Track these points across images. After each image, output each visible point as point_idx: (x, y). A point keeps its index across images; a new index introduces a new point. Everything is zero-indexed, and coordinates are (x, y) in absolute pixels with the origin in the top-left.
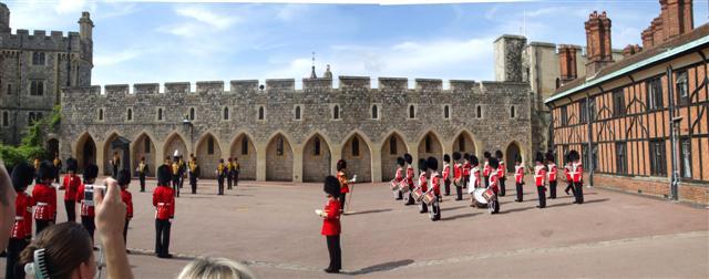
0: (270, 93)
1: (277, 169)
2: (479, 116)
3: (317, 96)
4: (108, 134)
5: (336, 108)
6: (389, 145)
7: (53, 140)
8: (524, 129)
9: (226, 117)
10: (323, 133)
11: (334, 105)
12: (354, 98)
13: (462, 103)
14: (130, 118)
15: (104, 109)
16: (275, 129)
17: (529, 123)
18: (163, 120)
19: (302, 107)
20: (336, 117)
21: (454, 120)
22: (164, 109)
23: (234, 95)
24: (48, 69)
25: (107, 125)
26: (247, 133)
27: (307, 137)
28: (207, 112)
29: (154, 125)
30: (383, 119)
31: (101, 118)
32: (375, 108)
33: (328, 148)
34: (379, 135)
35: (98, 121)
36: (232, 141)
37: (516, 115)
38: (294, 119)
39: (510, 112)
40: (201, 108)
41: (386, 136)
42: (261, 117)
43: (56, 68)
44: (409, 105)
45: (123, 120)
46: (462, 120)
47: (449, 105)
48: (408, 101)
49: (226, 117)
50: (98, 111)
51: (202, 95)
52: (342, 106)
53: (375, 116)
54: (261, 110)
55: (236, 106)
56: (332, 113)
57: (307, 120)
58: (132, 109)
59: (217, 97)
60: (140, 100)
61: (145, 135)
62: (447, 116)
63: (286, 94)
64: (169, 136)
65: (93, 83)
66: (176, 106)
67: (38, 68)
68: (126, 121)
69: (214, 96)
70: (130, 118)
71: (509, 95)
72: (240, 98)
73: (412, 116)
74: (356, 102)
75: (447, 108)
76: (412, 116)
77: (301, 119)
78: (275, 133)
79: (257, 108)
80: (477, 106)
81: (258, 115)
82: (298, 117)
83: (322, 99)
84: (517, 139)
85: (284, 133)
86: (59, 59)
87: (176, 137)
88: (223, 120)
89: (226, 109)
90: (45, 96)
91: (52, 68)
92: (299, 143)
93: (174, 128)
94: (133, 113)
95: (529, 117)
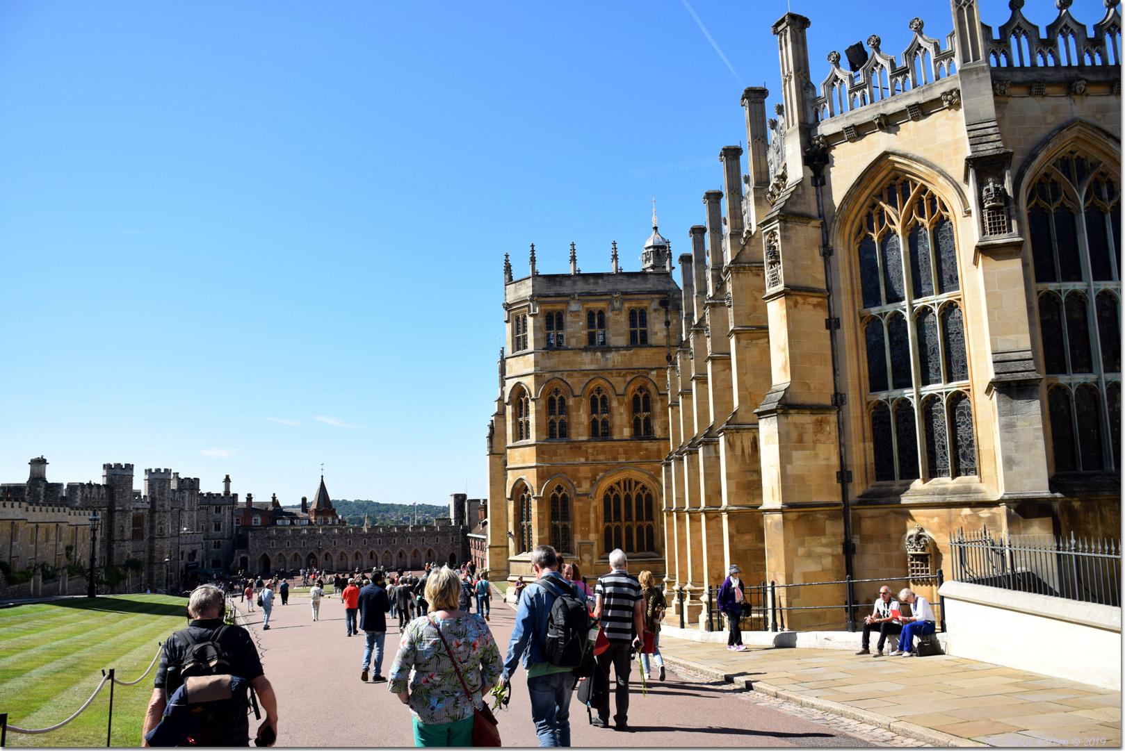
0: (353, 534)
4: (277, 554)
7: (244, 557)
8: (457, 547)
9: (335, 544)
10: (375, 550)
14: (288, 545)
15: (274, 542)
18: (306, 546)
19: (367, 540)
21: (426, 544)
24: (224, 515)
25: (276, 549)
27: (369, 552)
31: (273, 545)
40: (323, 541)
41: (398, 551)
48: (407, 536)
49: (335, 544)
62: (423, 542)
63: (360, 535)
65: (99, 478)
70: (288, 545)
73: (409, 542)
76: (409, 542)
79: (348, 540)
84: (454, 552)
85: (359, 551)
89: (335, 542)
90: (222, 531)
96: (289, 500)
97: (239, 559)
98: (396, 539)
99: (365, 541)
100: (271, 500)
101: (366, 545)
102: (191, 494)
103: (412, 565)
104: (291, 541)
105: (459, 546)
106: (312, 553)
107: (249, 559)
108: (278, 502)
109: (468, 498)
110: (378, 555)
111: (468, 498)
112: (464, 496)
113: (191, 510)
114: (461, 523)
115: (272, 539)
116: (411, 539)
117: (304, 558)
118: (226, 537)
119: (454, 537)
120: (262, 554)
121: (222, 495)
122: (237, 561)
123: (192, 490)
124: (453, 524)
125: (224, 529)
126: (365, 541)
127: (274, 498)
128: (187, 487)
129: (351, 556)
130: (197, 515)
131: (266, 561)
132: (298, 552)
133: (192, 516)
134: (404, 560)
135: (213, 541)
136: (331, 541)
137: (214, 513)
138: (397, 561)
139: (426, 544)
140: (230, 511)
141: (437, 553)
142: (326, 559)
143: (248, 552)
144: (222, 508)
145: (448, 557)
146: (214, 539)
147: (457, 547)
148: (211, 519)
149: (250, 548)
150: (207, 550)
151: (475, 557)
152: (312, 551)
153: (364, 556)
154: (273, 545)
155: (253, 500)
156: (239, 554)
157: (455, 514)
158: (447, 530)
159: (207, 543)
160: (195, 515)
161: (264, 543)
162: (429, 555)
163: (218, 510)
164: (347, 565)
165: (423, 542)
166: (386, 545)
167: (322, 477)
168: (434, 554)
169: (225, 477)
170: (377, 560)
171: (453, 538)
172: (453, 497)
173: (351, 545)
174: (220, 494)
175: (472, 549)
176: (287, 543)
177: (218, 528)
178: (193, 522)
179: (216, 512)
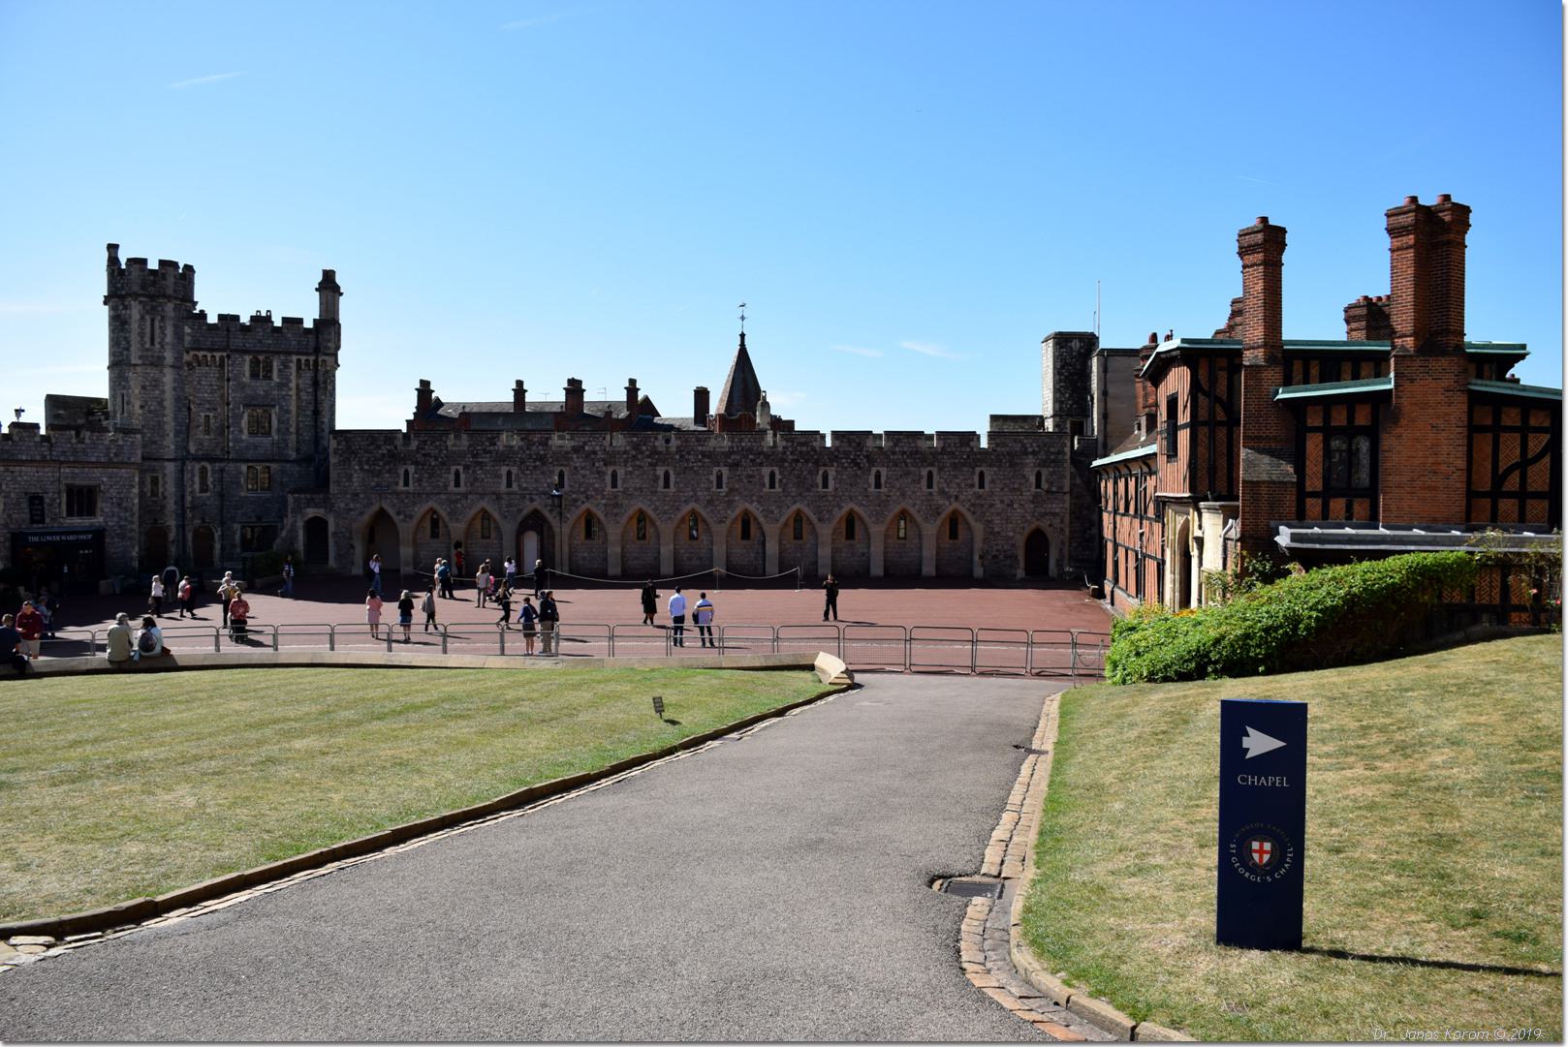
0: (679, 450)
1: (689, 559)
2: (982, 486)
3: (746, 457)
4: (420, 510)
5: (772, 475)
6: (844, 526)
8: (1056, 507)
9: (614, 485)
10: (754, 508)
11: (769, 469)
12: (797, 461)
13: (955, 466)
14: (457, 484)
16: (686, 502)
17: (1067, 497)
18: (515, 487)
20: (772, 486)
21: (942, 492)
22: (514, 470)
23: (625, 452)
26: (644, 508)
27: (734, 514)
28: (584, 476)
29: (498, 496)
30: (836, 489)
31: (406, 484)
32: (825, 477)
33: (761, 528)
34: (830, 511)
35: (401, 487)
36: (624, 520)
37: (1044, 485)
38: (714, 489)
39: (1033, 479)
41: (840, 514)
42: (667, 485)
43: (293, 385)
44: (874, 470)
45: (446, 486)
46: (953, 491)
47: (935, 470)
49: (614, 485)
50: (401, 472)
51: (576, 450)
52: (780, 473)
53: (825, 485)
54: (667, 475)
55: (631, 469)
56: (767, 480)
57: (732, 490)
58: (461, 468)
59: (600, 455)
60: (475, 456)
61: (484, 511)
62: (930, 485)
63: (703, 454)
64: (525, 512)
66: (535, 467)
67: (260, 387)
68: (452, 487)
69: (595, 453)
70: (457, 484)
71: (1034, 453)
72: (634, 456)
73: (878, 485)
74: (800, 465)
75: (930, 475)
77: (725, 489)
78: (686, 509)
79: (660, 471)
80: (978, 470)
81: (661, 482)
82: (719, 485)
83: (752, 461)
84: (1044, 524)
86: (299, 368)
87: (536, 514)
88: (609, 488)
89: (614, 475)
91: (286, 385)
92: (721, 522)
93: (532, 500)
94: (463, 476)
95: (1067, 489)
96: (674, 407)
97: (300, 524)
98: (832, 473)
99: (719, 477)
100: (623, 397)
101: (725, 489)
102: (152, 310)
103: (886, 569)
104: (466, 467)
105: (1063, 506)
106: (536, 512)
107: (331, 528)
108: (647, 399)
109: (1104, 344)
110: (766, 527)
111: (1104, 344)
112: (1090, 340)
113: (152, 364)
114: (1079, 428)
115: (403, 460)
116: (884, 471)
117: (508, 528)
118: (293, 455)
119: (1045, 472)
120: (375, 508)
121: (308, 324)
122: (293, 530)
123: (152, 297)
124: (1051, 430)
125: (284, 431)
126: (719, 477)
127: (632, 389)
128: (136, 288)
129: (723, 528)
130: (180, 383)
131: (380, 529)
132: (489, 509)
133: (157, 384)
134: (860, 548)
135: (244, 468)
136: (601, 474)
137: (247, 378)
138: (835, 551)
139: (942, 492)
140: (309, 374)
141: (978, 528)
142: (589, 535)
143: (327, 504)
144: (275, 364)
145: (1020, 541)
146: (246, 461)
147: (1056, 507)
148: (233, 396)
149: (333, 488)
150: (222, 496)
151: (1116, 546)
152: (536, 505)
153: (715, 528)
154: (406, 484)
155: (587, 397)
156: (298, 510)
157: (1056, 400)
158: (1018, 447)
159: (222, 470)
160: (168, 378)
161: (379, 474)
162: (954, 535)
163: (261, 371)
164: (657, 559)
165: (930, 485)
166: (793, 490)
167: (743, 336)
168: (970, 528)
169: (320, 278)
170: (764, 544)
171: (1038, 476)
172: (1051, 343)
173: (672, 488)
174: (300, 321)
175: (1105, 515)
176: (452, 477)
177: (259, 427)
178: (161, 403)
179: (254, 375)
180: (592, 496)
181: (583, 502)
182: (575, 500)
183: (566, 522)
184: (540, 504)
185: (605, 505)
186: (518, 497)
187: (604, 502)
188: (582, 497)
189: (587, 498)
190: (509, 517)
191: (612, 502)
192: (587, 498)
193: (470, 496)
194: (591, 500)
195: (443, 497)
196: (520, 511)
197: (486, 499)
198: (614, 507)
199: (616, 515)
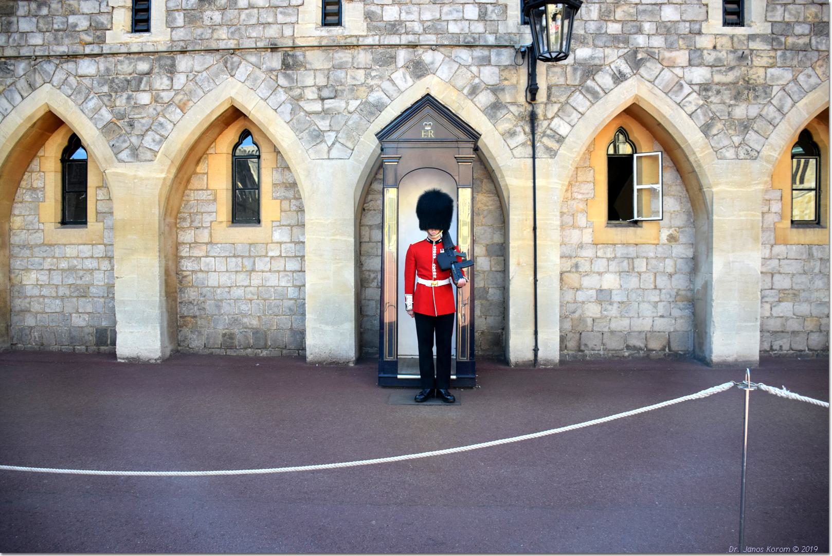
93: (418, 70)
180: (651, 55)
181: (619, 78)
182: (590, 70)
183: (552, 153)
184: (450, 82)
185: (705, 88)
186: (364, 57)
187: (699, 74)
188: (615, 58)
189: (636, 63)
190: (330, 137)
191: (730, 77)
192: (636, 63)
193: (183, 63)
194: (650, 69)
195: (87, 67)
196: (379, 107)
197: (243, 70)
198: (737, 96)
199: (745, 126)
